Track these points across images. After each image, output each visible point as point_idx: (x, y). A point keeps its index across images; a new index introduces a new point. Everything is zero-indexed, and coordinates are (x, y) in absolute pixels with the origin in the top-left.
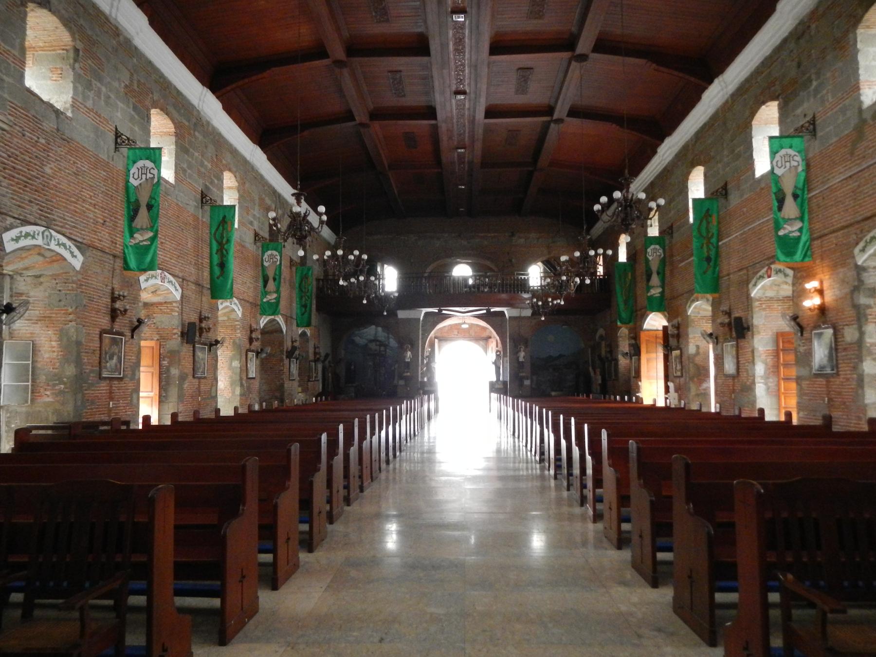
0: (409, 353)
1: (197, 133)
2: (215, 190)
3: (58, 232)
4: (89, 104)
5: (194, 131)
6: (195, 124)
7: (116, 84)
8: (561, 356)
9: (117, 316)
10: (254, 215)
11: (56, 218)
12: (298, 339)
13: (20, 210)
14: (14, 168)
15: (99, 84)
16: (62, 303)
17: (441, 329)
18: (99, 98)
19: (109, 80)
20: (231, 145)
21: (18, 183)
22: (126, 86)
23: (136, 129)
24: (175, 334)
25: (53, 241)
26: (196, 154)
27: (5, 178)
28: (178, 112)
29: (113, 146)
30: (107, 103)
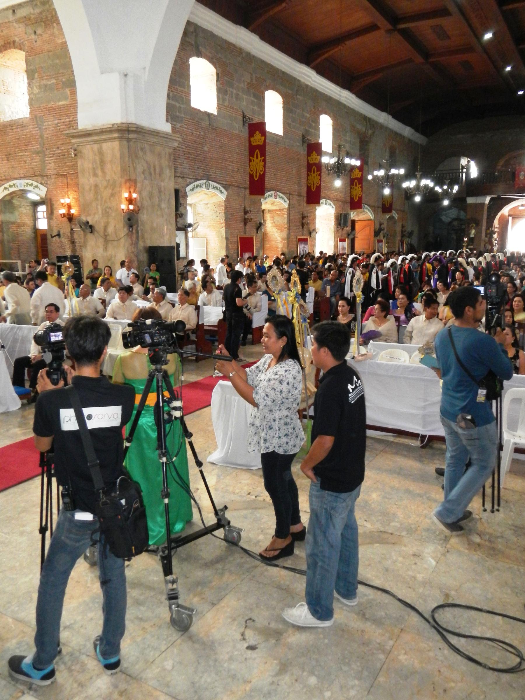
0: (473, 231)
1: (298, 97)
2: (313, 131)
3: (213, 181)
4: (226, 103)
6: (297, 91)
7: (242, 85)
11: (211, 173)
13: (193, 174)
14: (189, 152)
15: (231, 90)
16: (218, 218)
17: (514, 208)
18: (232, 97)
19: (237, 84)
21: (191, 160)
22: (248, 84)
23: (256, 108)
26: (298, 111)
29: (241, 123)
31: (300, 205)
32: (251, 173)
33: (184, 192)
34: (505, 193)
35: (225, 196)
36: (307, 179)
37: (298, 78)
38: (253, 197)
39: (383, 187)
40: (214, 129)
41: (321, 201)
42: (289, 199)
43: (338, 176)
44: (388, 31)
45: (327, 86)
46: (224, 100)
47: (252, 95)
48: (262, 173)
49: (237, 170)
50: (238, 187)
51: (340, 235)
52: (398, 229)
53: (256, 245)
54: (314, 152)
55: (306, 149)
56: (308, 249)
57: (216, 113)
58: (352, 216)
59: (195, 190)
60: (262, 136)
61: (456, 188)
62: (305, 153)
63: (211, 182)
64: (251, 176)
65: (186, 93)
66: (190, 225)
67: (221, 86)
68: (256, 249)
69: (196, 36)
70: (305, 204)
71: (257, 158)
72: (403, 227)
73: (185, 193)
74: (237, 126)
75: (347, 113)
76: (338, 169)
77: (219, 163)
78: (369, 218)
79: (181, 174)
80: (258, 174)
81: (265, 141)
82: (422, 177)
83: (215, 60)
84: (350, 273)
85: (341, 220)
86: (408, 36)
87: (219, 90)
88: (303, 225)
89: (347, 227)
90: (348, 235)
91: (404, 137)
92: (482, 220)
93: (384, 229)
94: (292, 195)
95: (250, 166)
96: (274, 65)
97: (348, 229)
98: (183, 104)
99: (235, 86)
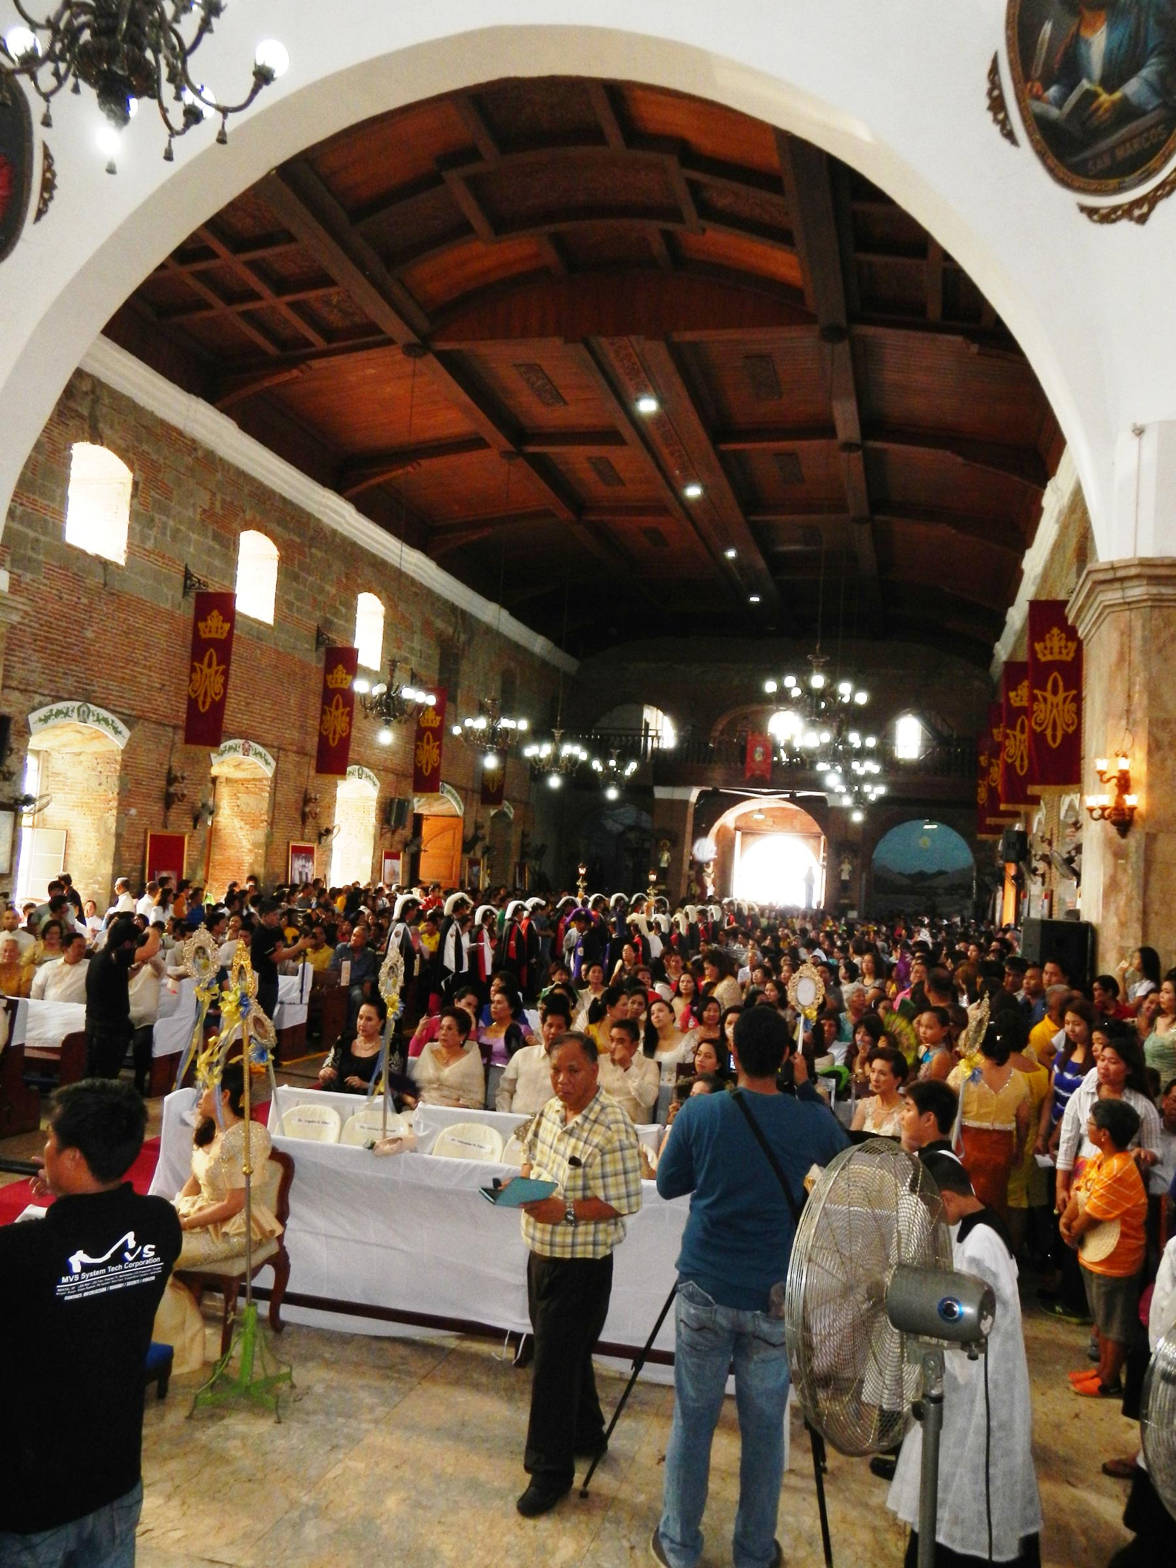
0: (666, 856)
1: (314, 550)
2: (342, 622)
4: (149, 545)
5: (310, 547)
7: (190, 513)
8: (941, 873)
9: (173, 802)
10: (413, 648)
11: (96, 688)
12: (488, 824)
13: (51, 686)
14: (46, 637)
15: (164, 518)
16: (103, 787)
17: (745, 815)
18: (164, 534)
20: (374, 556)
22: (204, 511)
23: (217, 562)
24: (262, 821)
25: (91, 718)
26: (311, 579)
27: (34, 650)
28: (286, 528)
29: (181, 590)
30: (174, 539)
31: (299, 773)
32: (193, 696)
33: (22, 723)
34: (728, 785)
35: (125, 741)
36: (322, 722)
37: (317, 515)
38: (192, 748)
39: (484, 753)
40: (113, 594)
41: (349, 769)
42: (277, 759)
43: (388, 722)
44: (505, 454)
45: (378, 538)
46: (144, 538)
47: (210, 535)
48: (217, 698)
49: (158, 686)
50: (160, 724)
51: (387, 843)
52: (515, 839)
53: (189, 853)
54: (340, 667)
55: (323, 657)
56: (311, 871)
57: (122, 562)
58: (416, 806)
59: (51, 722)
60: (223, 621)
61: (633, 766)
62: (321, 665)
63: (92, 707)
64: (192, 703)
65: (54, 511)
66: (28, 800)
67: (140, 508)
68: (189, 863)
69: (96, 401)
70: (312, 773)
71: (210, 665)
72: (524, 835)
73: (27, 725)
74: (170, 594)
75: (416, 594)
76: (388, 708)
77: (117, 667)
78: (453, 813)
79: (20, 683)
80: (209, 700)
81: (230, 632)
82: (564, 739)
83: (132, 456)
84: (397, 935)
85: (391, 810)
86: (544, 468)
87: (134, 515)
88: (304, 817)
89: (404, 828)
90: (406, 845)
91: (533, 654)
92: (684, 836)
93: (483, 838)
94: (284, 750)
95: (191, 681)
96: (266, 483)
97: (406, 832)
98: (45, 533)
99: (173, 512)
